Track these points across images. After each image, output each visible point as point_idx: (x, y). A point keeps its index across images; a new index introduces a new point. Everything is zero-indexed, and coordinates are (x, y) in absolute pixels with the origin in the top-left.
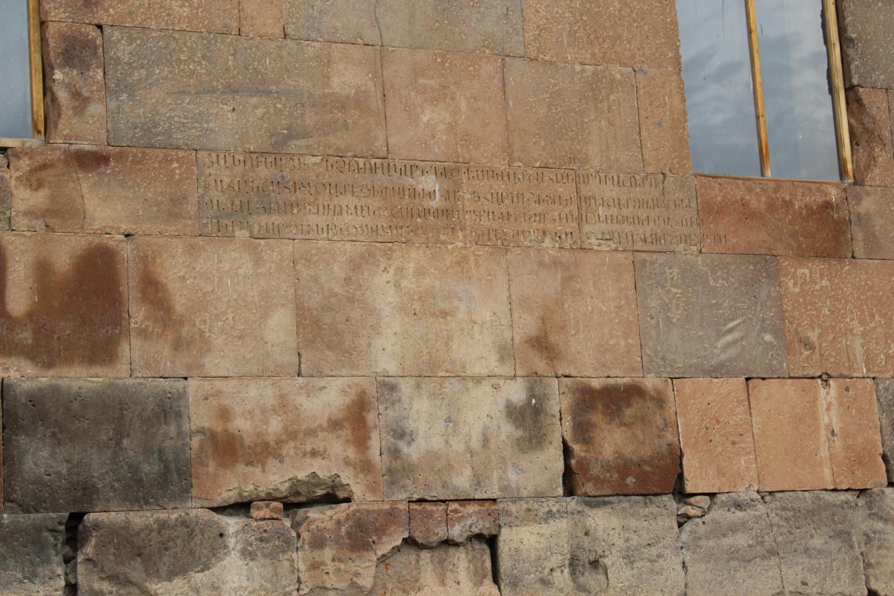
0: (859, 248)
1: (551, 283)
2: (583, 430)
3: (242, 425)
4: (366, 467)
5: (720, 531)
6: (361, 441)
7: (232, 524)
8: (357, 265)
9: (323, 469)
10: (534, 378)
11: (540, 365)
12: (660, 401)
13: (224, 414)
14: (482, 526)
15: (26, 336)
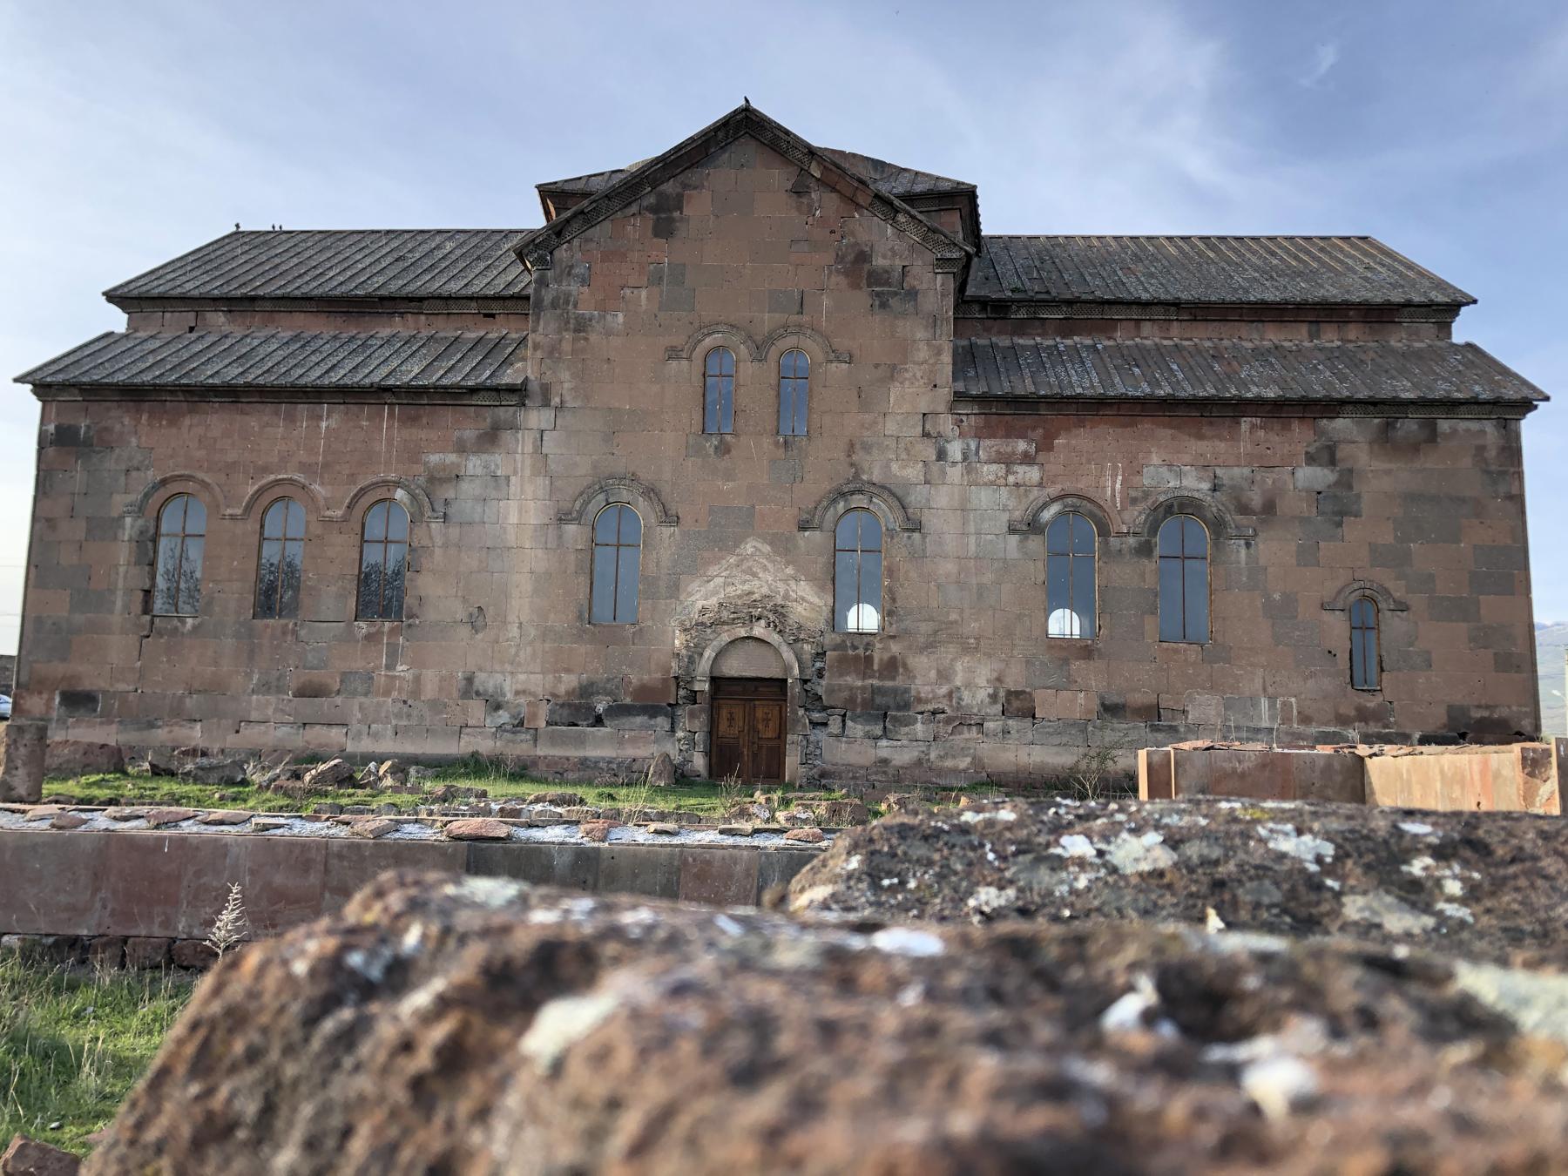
0: (1096, 657)
1: (1002, 666)
2: (1008, 701)
3: (923, 695)
4: (951, 706)
5: (1044, 727)
6: (951, 701)
7: (919, 716)
8: (952, 660)
9: (941, 706)
10: (996, 689)
11: (998, 684)
12: (1030, 694)
13: (919, 693)
14: (979, 721)
15: (877, 675)
